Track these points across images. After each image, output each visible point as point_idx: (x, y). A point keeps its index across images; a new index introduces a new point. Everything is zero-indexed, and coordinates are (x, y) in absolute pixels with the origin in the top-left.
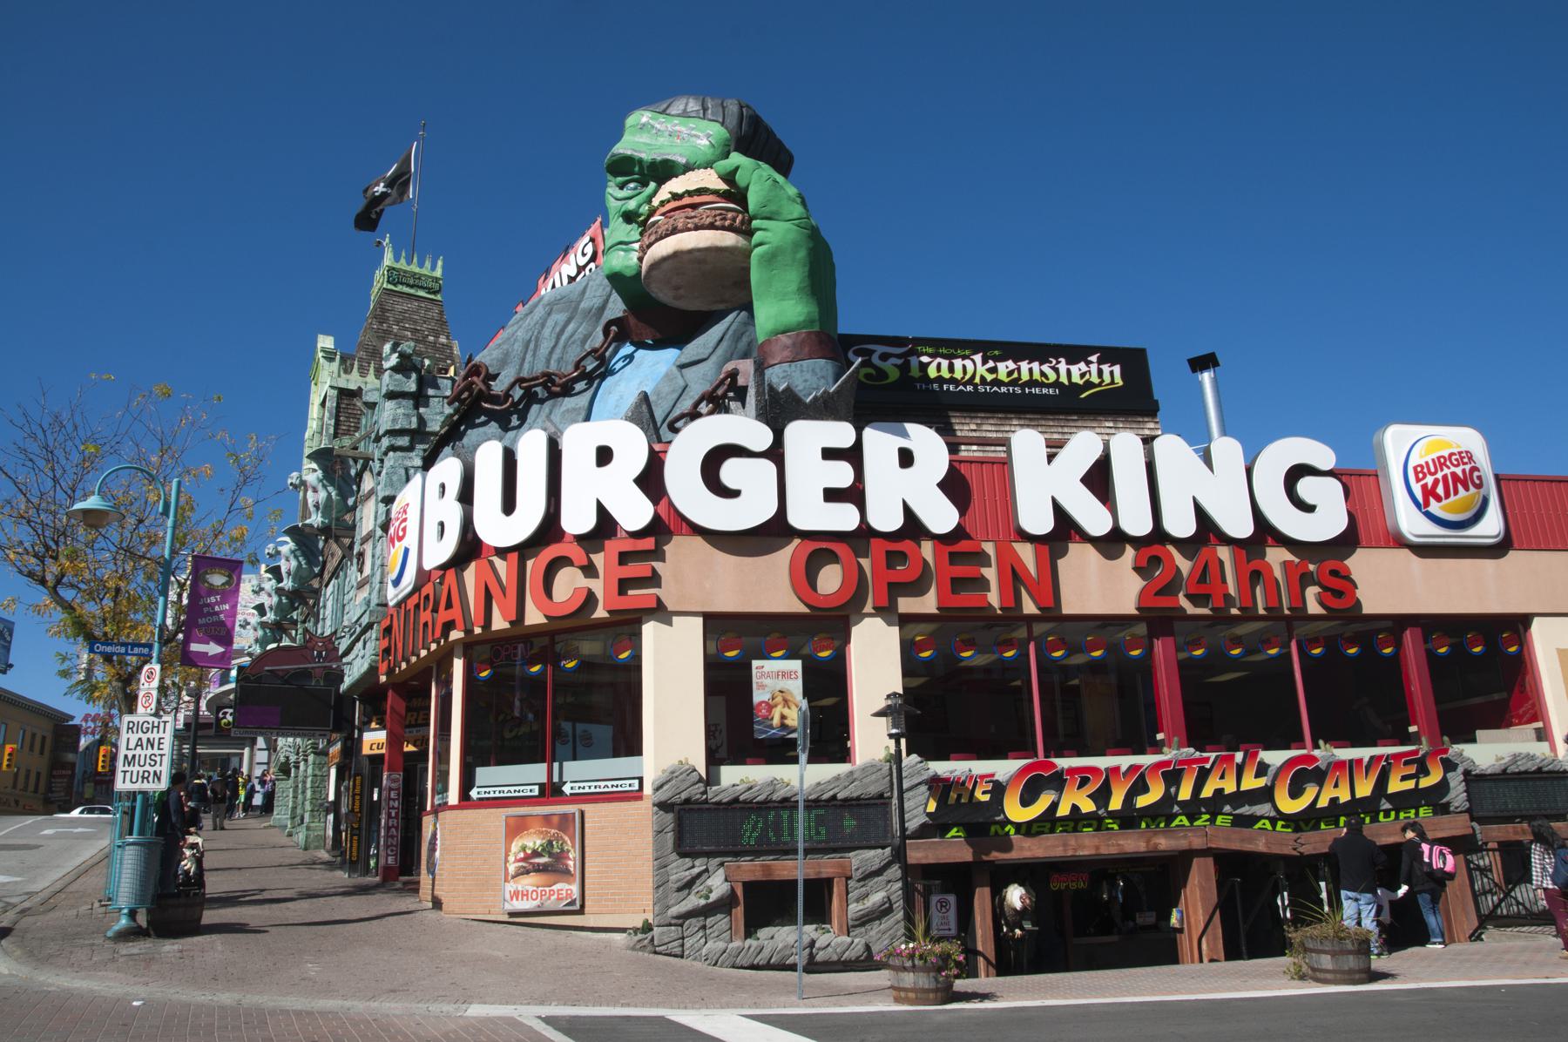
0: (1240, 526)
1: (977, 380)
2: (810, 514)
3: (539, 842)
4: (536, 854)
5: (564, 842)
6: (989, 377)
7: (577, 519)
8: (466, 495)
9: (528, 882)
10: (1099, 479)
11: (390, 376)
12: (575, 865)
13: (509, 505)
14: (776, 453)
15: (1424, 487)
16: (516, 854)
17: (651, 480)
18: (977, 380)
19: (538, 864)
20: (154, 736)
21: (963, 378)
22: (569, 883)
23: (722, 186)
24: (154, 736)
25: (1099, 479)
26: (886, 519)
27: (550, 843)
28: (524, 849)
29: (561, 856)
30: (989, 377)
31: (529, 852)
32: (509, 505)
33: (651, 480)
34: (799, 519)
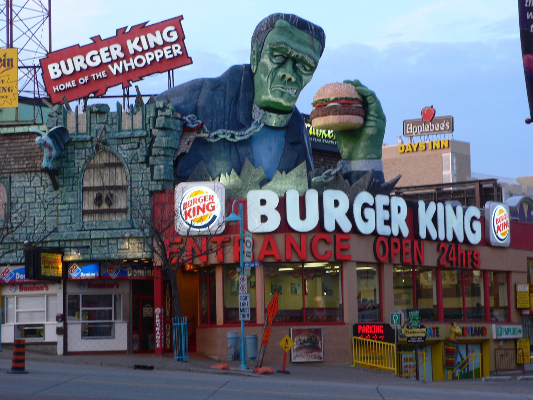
0: (461, 239)
1: (322, 137)
2: (383, 230)
3: (306, 338)
4: (305, 342)
5: (317, 338)
6: (326, 136)
7: (329, 226)
8: (282, 207)
9: (302, 352)
10: (435, 220)
11: (165, 120)
12: (321, 346)
13: (303, 216)
14: (374, 207)
15: (498, 226)
16: (297, 342)
17: (350, 215)
18: (322, 137)
19: (306, 346)
20: (246, 301)
21: (318, 135)
22: (319, 352)
23: (359, 97)
24: (246, 301)
25: (435, 220)
26: (396, 233)
27: (311, 338)
28: (300, 340)
29: (316, 342)
30: (326, 136)
31: (302, 341)
32: (303, 216)
33: (350, 215)
34: (380, 231)
